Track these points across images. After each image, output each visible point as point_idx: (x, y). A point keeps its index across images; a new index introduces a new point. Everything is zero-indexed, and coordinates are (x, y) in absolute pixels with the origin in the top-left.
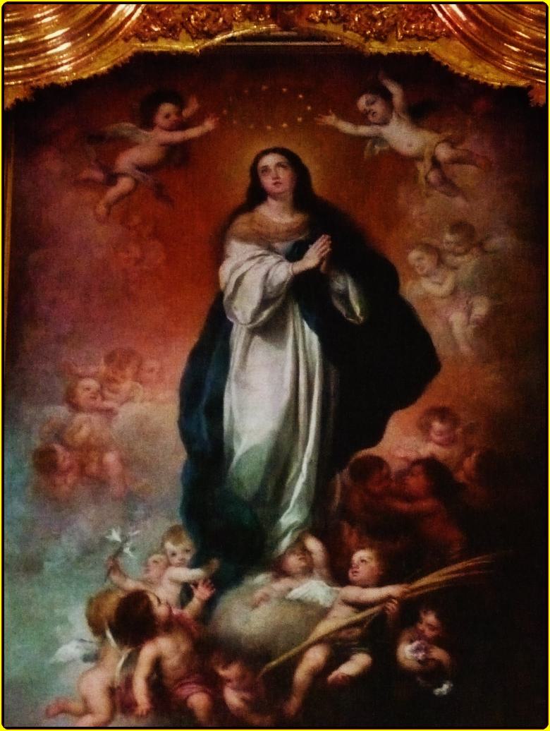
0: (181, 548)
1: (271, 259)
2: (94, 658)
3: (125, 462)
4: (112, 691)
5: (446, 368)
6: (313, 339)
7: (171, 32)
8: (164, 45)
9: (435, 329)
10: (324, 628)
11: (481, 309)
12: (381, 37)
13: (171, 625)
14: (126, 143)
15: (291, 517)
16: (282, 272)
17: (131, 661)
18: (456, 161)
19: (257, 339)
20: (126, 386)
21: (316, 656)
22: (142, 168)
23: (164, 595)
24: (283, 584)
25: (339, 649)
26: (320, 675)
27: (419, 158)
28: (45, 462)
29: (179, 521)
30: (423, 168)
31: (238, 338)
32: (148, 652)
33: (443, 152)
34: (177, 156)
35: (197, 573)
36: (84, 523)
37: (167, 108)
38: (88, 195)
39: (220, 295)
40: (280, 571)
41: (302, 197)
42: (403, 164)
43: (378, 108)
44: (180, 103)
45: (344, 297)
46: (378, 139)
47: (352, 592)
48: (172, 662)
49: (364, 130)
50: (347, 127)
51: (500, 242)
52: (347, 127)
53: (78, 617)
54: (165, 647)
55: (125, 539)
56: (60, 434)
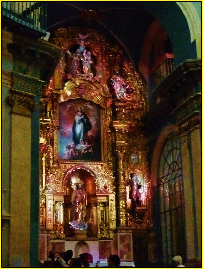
0: (72, 142)
1: (79, 117)
2: (66, 150)
5: (93, 128)
6: (82, 124)
8: (71, 98)
9: (92, 124)
10: (84, 149)
12: (89, 99)
13: (72, 148)
14: (68, 106)
15: (81, 140)
16: (80, 118)
17: (69, 151)
21: (83, 151)
23: (71, 145)
25: (85, 150)
26: (83, 152)
27: (91, 109)
28: (62, 134)
31: (77, 124)
34: (72, 107)
35: (73, 144)
37: (71, 103)
40: (80, 144)
41: (81, 112)
42: (89, 109)
43: (88, 104)
47: (86, 146)
49: (86, 106)
53: (65, 148)
54: (71, 150)
56: (63, 131)
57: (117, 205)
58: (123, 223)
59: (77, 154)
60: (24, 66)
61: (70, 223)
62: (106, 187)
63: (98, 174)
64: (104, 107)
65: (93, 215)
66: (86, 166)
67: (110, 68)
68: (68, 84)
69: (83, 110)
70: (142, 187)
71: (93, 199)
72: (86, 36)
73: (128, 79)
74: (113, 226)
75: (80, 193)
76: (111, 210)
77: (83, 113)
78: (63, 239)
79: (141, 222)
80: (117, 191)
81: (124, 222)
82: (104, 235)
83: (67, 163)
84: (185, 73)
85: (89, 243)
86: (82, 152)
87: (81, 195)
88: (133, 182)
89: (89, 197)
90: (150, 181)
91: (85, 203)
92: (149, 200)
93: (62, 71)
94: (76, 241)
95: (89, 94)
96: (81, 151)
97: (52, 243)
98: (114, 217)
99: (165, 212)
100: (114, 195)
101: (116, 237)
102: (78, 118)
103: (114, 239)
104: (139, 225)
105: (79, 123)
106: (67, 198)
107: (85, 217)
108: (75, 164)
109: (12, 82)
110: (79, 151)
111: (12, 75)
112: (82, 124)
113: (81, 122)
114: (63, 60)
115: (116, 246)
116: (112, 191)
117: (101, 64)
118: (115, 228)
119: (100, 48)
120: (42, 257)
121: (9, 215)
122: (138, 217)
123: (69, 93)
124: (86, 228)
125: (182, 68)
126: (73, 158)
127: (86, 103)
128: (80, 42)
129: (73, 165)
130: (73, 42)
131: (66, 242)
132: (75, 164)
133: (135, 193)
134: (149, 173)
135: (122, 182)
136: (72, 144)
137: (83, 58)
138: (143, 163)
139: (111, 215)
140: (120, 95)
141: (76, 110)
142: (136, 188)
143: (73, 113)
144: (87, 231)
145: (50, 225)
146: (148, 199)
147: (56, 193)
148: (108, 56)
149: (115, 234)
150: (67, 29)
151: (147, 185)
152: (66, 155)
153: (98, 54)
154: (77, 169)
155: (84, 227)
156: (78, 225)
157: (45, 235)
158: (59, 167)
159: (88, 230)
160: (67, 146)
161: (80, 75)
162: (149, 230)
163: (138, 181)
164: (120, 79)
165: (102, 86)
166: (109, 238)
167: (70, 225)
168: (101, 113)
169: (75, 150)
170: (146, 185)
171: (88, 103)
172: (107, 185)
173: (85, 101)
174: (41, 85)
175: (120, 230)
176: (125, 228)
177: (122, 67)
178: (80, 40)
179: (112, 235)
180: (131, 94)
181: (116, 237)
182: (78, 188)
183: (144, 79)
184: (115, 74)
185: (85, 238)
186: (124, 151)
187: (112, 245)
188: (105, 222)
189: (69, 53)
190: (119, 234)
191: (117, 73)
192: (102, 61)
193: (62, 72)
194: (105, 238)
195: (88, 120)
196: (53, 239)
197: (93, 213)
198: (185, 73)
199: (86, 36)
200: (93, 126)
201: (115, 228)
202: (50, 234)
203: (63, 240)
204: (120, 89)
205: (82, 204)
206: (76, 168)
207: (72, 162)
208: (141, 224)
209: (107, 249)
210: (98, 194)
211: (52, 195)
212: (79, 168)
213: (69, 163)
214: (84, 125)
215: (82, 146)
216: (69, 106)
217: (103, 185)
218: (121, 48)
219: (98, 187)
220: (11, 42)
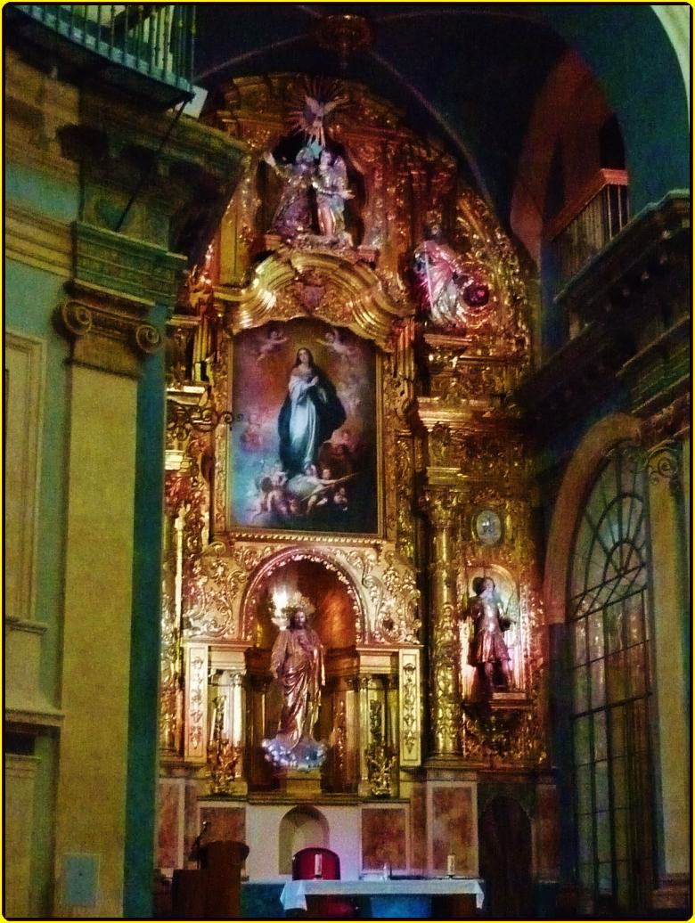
0: (279, 466)
1: (303, 382)
2: (257, 495)
3: (264, 440)
4: (262, 505)
6: (313, 407)
7: (279, 314)
8: (277, 318)
9: (346, 407)
10: (316, 491)
11: (358, 401)
12: (336, 321)
14: (265, 344)
15: (308, 459)
16: (306, 386)
17: (266, 497)
18: (351, 356)
20: (264, 417)
21: (313, 498)
22: (269, 352)
23: (274, 480)
24: (305, 478)
25: (319, 498)
28: (243, 439)
29: (278, 458)
30: (343, 357)
31: (294, 405)
32: (270, 495)
34: (277, 347)
35: (281, 474)
39: (289, 392)
40: (304, 474)
41: (311, 364)
42: (337, 356)
43: (331, 337)
44: (278, 332)
45: (321, 395)
46: (331, 347)
47: (323, 481)
48: (277, 498)
49: (327, 344)
51: (363, 381)
53: (252, 485)
54: (275, 494)
57: (428, 686)
58: (444, 748)
59: (293, 508)
60: (118, 203)
61: (264, 744)
62: (389, 624)
63: (363, 579)
64: (387, 350)
66: (323, 549)
67: (412, 214)
68: (265, 268)
70: (513, 626)
71: (344, 663)
72: (330, 106)
73: (473, 255)
74: (411, 755)
75: (302, 642)
77: (316, 370)
78: (240, 797)
79: (508, 747)
80: (426, 637)
81: (450, 745)
83: (259, 540)
84: (666, 234)
86: (310, 503)
87: (305, 649)
88: (482, 609)
89: (331, 656)
90: (540, 607)
91: (316, 677)
92: (536, 672)
93: (245, 225)
95: (336, 306)
96: (308, 499)
97: (206, 813)
98: (416, 727)
99: (590, 713)
100: (417, 652)
101: (421, 794)
102: (297, 385)
103: (412, 800)
104: (503, 756)
105: (302, 403)
106: (256, 658)
107: (317, 725)
108: (283, 541)
109: (74, 256)
110: (301, 501)
111: (74, 233)
112: (311, 407)
113: (309, 400)
114: (249, 185)
115: (420, 824)
118: (418, 763)
119: (380, 149)
120: (166, 856)
121: (53, 711)
123: (269, 299)
124: (320, 764)
126: (278, 522)
128: (310, 123)
129: (279, 547)
131: (248, 808)
132: (289, 541)
133: (487, 645)
134: (537, 576)
135: (446, 606)
136: (276, 473)
137: (320, 178)
138: (518, 543)
140: (442, 309)
142: (491, 627)
143: (280, 367)
144: (321, 771)
145: (196, 750)
146: (533, 667)
147: (221, 642)
149: (418, 785)
150: (267, 81)
151: (530, 618)
152: (256, 513)
154: (292, 561)
155: (314, 757)
156: (294, 751)
158: (229, 552)
159: (325, 768)
161: (306, 240)
162: (533, 774)
163: (499, 604)
164: (444, 255)
165: (381, 278)
166: (397, 798)
167: (265, 751)
168: (378, 371)
169: (287, 495)
170: (527, 620)
173: (322, 328)
175: (438, 770)
176: (454, 764)
177: (451, 212)
178: (311, 118)
179: (407, 789)
180: (481, 308)
181: (421, 794)
182: (294, 625)
184: (428, 237)
187: (406, 824)
188: (386, 746)
189: (271, 161)
190: (431, 786)
191: (435, 232)
192: (382, 192)
193: (246, 228)
194: (385, 797)
195: (332, 391)
198: (666, 234)
199: (330, 106)
200: (347, 413)
201: (418, 763)
202: (197, 779)
204: (445, 288)
205: (308, 680)
206: (290, 558)
208: (506, 754)
209: (389, 833)
210: (362, 645)
212: (299, 558)
213: (265, 540)
214: (319, 412)
215: (310, 483)
216: (268, 346)
217: (381, 616)
218: (450, 148)
219: (363, 623)
220: (72, 119)
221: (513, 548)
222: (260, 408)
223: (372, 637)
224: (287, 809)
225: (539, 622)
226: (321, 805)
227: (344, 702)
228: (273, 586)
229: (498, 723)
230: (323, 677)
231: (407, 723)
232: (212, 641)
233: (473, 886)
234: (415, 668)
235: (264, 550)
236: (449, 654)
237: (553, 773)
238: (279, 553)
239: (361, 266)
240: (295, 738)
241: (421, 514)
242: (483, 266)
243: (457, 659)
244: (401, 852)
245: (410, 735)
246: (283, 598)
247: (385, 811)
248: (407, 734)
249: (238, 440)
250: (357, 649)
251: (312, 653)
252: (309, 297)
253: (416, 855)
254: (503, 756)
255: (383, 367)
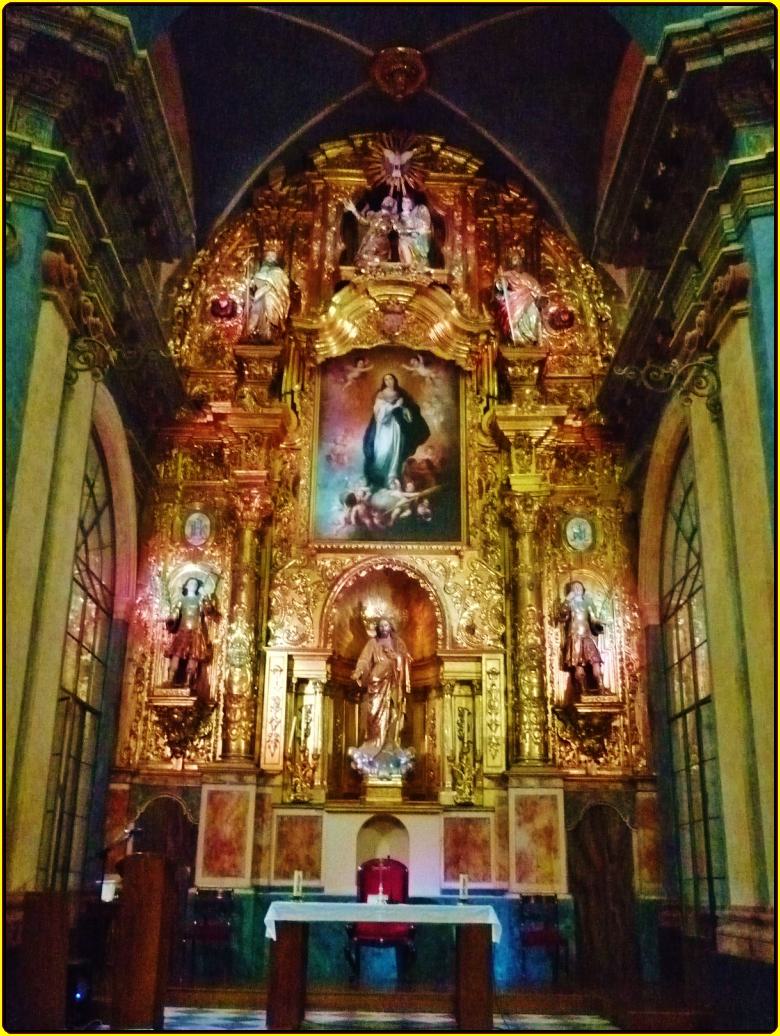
0: (363, 482)
1: (388, 404)
2: (341, 510)
3: (349, 459)
4: (346, 519)
6: (398, 426)
7: (362, 343)
8: (360, 347)
10: (400, 503)
11: (442, 419)
12: (417, 345)
13: (360, 502)
14: (349, 372)
15: (392, 474)
16: (391, 408)
17: (350, 511)
19: (384, 427)
20: (349, 438)
21: (397, 511)
22: (355, 379)
23: (359, 495)
25: (403, 510)
26: (398, 515)
28: (329, 458)
30: (428, 380)
31: (379, 425)
32: (355, 509)
33: (433, 376)
34: (363, 375)
36: (339, 475)
38: (339, 386)
40: (389, 489)
41: (396, 387)
42: (422, 379)
43: (416, 362)
46: (416, 372)
49: (412, 369)
50: (408, 368)
51: (448, 400)
52: (408, 368)
54: (359, 508)
55: (349, 479)
56: (333, 451)
57: (515, 691)
58: (529, 753)
59: (376, 521)
62: (471, 629)
64: (468, 369)
65: (434, 724)
66: (405, 558)
67: (493, 250)
68: (343, 298)
69: (400, 384)
70: (606, 629)
71: (430, 673)
72: (407, 156)
74: (495, 762)
75: (386, 650)
76: (491, 707)
77: (400, 392)
78: (320, 804)
79: (602, 750)
81: (536, 751)
82: (464, 796)
84: (671, 94)
85: (403, 819)
86: (393, 516)
87: (388, 657)
89: (416, 667)
90: (635, 610)
91: (400, 684)
92: (633, 676)
94: (359, 816)
96: (390, 514)
97: (282, 821)
98: (501, 733)
99: (683, 714)
100: (501, 657)
101: (504, 801)
102: (383, 407)
104: (598, 763)
105: (387, 423)
106: (341, 665)
110: (385, 513)
112: (396, 426)
115: (504, 835)
116: (491, 643)
117: (459, 237)
119: (458, 192)
120: (234, 866)
122: (588, 732)
123: (352, 332)
124: (404, 771)
125: (659, 73)
126: (364, 532)
127: (412, 361)
129: (359, 557)
130: (370, 178)
131: (326, 816)
132: (368, 551)
136: (360, 488)
137: (401, 221)
138: (609, 548)
139: (490, 726)
141: (379, 386)
142: (581, 630)
143: (366, 392)
144: (402, 779)
145: (272, 757)
146: (630, 670)
147: (299, 650)
148: (492, 220)
149: (503, 793)
150: (351, 143)
151: (624, 622)
152: (339, 527)
153: (450, 210)
154: (373, 570)
155: (398, 764)
156: (375, 758)
157: (251, 791)
159: (409, 777)
160: (345, 496)
162: (632, 782)
163: (590, 608)
164: (523, 282)
165: (457, 300)
167: (350, 759)
169: (370, 508)
170: (621, 623)
171: (418, 360)
172: (477, 622)
173: (407, 354)
174: (47, 170)
175: (519, 777)
176: (541, 771)
177: (533, 246)
178: (390, 168)
181: (504, 801)
182: (380, 635)
183: (614, 283)
184: (509, 267)
185: (395, 803)
186: (536, 508)
187: (491, 831)
188: (471, 749)
189: (351, 207)
191: (515, 262)
192: (463, 231)
194: (467, 805)
195: (416, 411)
196: (284, 805)
197: (434, 719)
199: (407, 156)
200: (431, 429)
201: (504, 769)
202: (272, 786)
203: (317, 809)
206: (371, 567)
207: (366, 546)
208: (601, 760)
209: (475, 845)
211: (285, 655)
212: (380, 567)
215: (395, 497)
217: (464, 623)
218: (527, 188)
221: (606, 554)
222: (346, 431)
223: (454, 642)
224: (366, 817)
225: (634, 626)
226: (402, 813)
227: (434, 709)
228: (366, 598)
229: (588, 726)
230: (408, 682)
231: (491, 729)
232: (292, 650)
233: (487, 911)
234: (499, 673)
235: (346, 560)
236: (532, 656)
237: (652, 780)
238: (359, 563)
239: (434, 289)
240: (378, 745)
241: (507, 521)
242: (567, 294)
243: (542, 662)
244: (487, 863)
245: (494, 740)
246: (377, 607)
247: (469, 821)
248: (491, 739)
249: (324, 460)
250: (439, 655)
251: (396, 660)
252: (388, 324)
253: (501, 867)
254: (598, 763)
255: (466, 385)
